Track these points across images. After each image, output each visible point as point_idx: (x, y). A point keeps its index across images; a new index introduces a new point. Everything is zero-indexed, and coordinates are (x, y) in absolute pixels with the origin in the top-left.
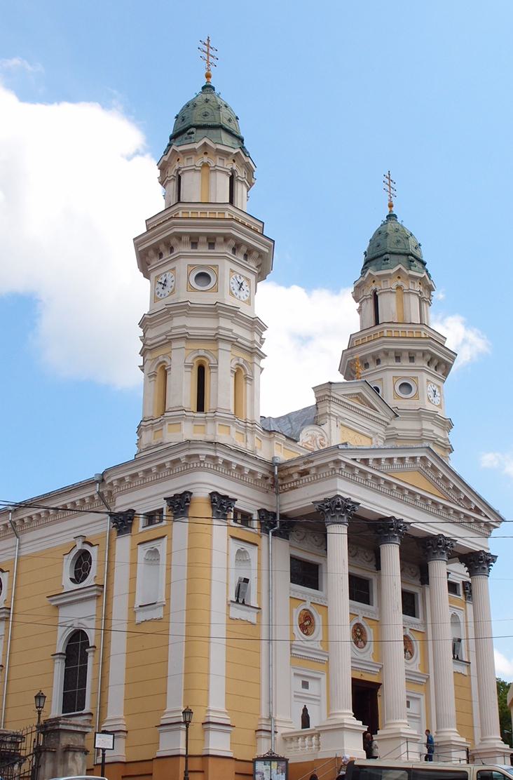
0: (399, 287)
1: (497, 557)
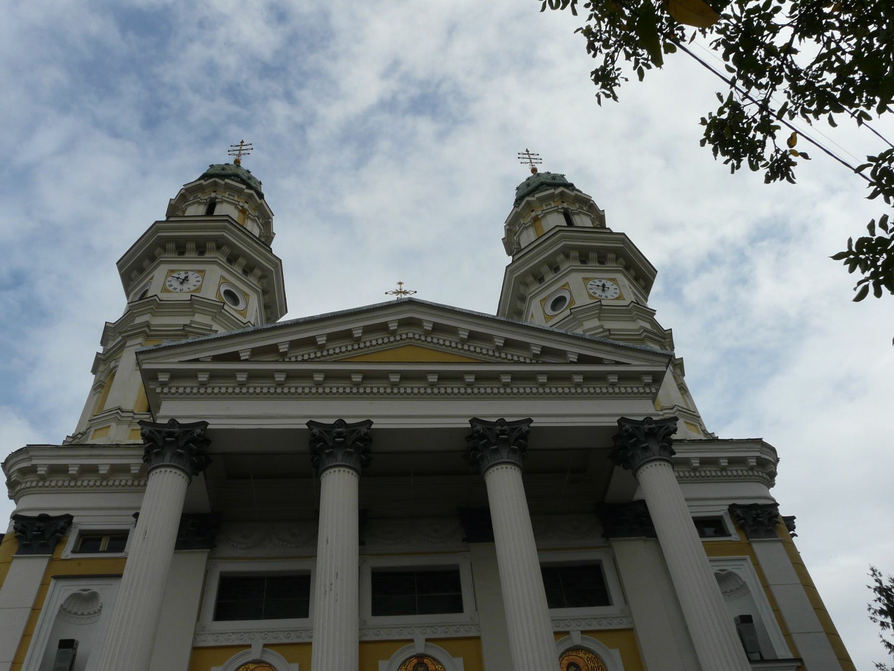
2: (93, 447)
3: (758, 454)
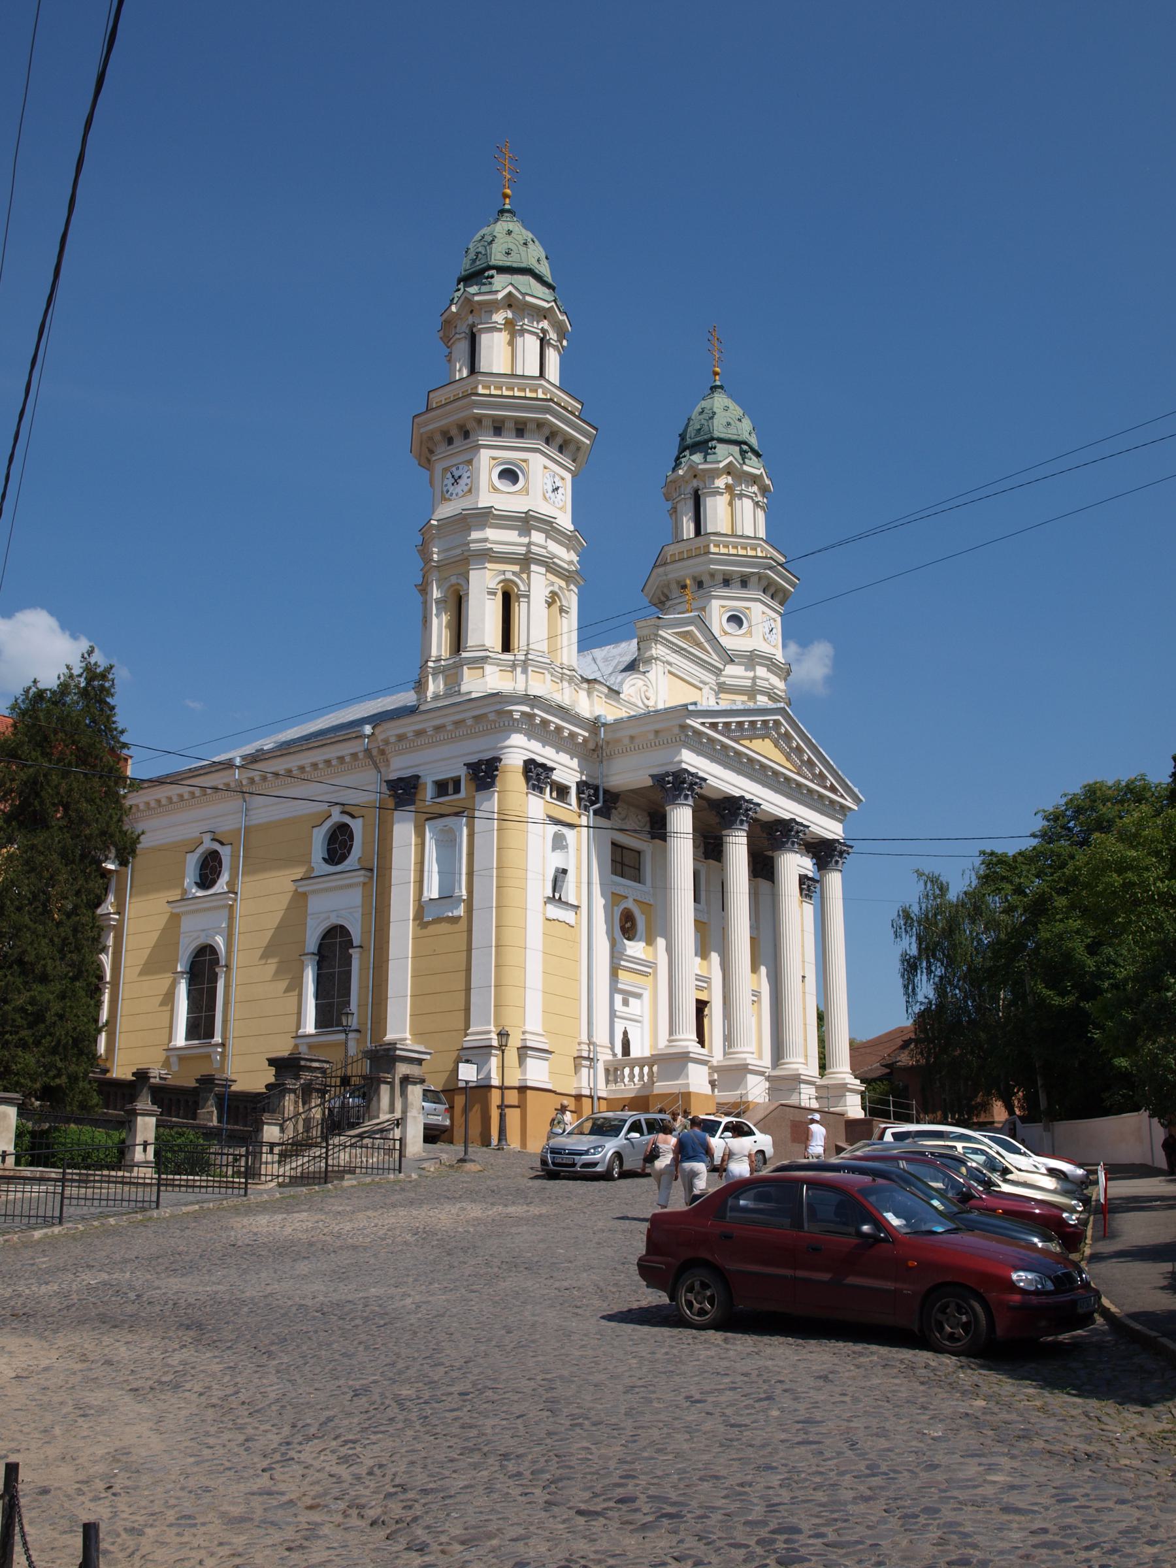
0: (728, 487)
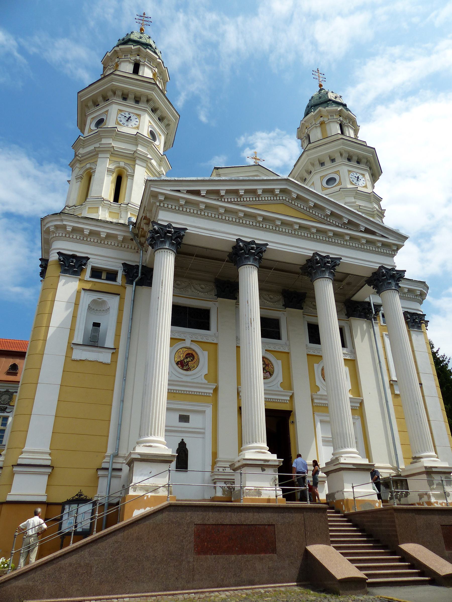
1: (405, 271)
2: (97, 221)
3: (422, 289)
